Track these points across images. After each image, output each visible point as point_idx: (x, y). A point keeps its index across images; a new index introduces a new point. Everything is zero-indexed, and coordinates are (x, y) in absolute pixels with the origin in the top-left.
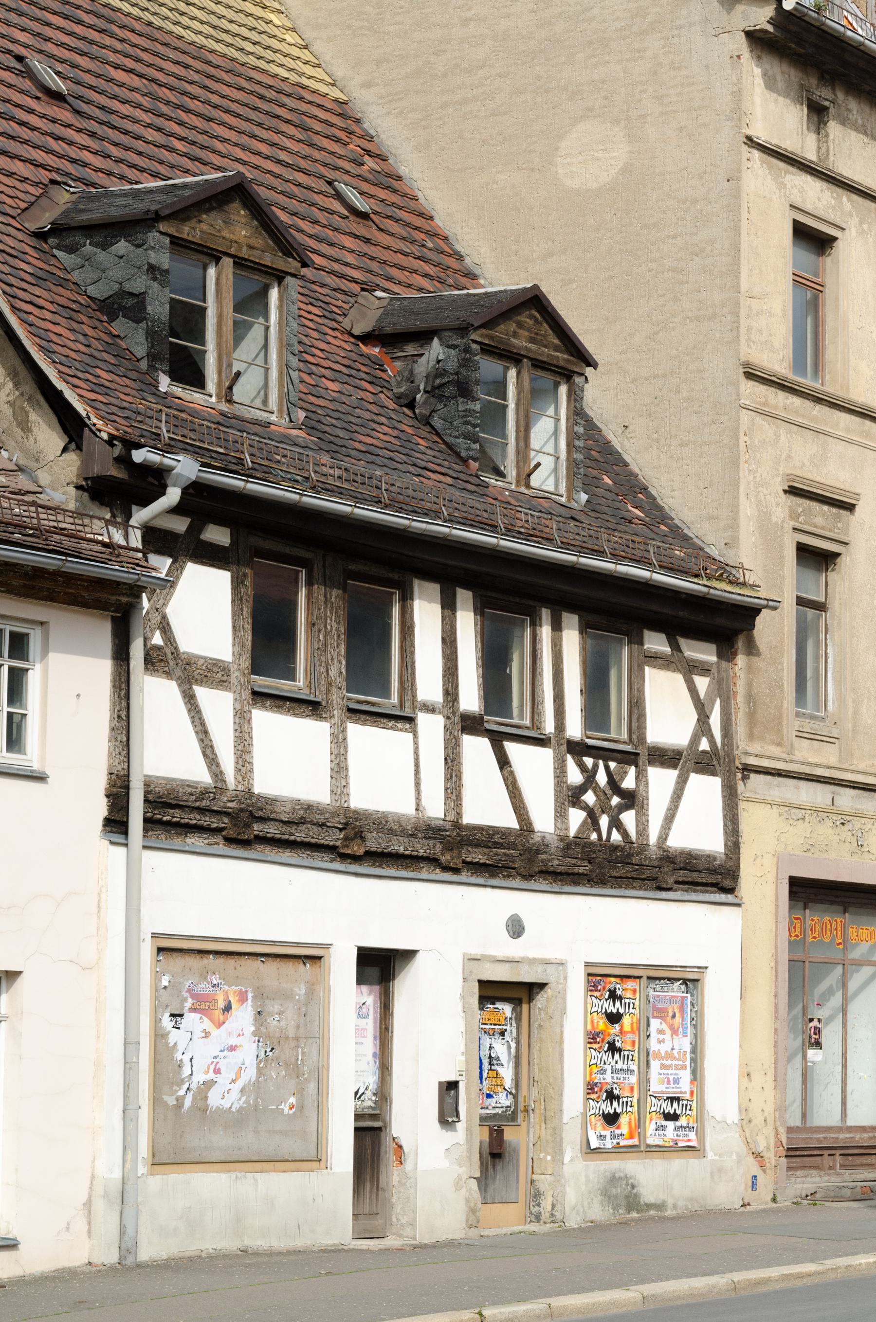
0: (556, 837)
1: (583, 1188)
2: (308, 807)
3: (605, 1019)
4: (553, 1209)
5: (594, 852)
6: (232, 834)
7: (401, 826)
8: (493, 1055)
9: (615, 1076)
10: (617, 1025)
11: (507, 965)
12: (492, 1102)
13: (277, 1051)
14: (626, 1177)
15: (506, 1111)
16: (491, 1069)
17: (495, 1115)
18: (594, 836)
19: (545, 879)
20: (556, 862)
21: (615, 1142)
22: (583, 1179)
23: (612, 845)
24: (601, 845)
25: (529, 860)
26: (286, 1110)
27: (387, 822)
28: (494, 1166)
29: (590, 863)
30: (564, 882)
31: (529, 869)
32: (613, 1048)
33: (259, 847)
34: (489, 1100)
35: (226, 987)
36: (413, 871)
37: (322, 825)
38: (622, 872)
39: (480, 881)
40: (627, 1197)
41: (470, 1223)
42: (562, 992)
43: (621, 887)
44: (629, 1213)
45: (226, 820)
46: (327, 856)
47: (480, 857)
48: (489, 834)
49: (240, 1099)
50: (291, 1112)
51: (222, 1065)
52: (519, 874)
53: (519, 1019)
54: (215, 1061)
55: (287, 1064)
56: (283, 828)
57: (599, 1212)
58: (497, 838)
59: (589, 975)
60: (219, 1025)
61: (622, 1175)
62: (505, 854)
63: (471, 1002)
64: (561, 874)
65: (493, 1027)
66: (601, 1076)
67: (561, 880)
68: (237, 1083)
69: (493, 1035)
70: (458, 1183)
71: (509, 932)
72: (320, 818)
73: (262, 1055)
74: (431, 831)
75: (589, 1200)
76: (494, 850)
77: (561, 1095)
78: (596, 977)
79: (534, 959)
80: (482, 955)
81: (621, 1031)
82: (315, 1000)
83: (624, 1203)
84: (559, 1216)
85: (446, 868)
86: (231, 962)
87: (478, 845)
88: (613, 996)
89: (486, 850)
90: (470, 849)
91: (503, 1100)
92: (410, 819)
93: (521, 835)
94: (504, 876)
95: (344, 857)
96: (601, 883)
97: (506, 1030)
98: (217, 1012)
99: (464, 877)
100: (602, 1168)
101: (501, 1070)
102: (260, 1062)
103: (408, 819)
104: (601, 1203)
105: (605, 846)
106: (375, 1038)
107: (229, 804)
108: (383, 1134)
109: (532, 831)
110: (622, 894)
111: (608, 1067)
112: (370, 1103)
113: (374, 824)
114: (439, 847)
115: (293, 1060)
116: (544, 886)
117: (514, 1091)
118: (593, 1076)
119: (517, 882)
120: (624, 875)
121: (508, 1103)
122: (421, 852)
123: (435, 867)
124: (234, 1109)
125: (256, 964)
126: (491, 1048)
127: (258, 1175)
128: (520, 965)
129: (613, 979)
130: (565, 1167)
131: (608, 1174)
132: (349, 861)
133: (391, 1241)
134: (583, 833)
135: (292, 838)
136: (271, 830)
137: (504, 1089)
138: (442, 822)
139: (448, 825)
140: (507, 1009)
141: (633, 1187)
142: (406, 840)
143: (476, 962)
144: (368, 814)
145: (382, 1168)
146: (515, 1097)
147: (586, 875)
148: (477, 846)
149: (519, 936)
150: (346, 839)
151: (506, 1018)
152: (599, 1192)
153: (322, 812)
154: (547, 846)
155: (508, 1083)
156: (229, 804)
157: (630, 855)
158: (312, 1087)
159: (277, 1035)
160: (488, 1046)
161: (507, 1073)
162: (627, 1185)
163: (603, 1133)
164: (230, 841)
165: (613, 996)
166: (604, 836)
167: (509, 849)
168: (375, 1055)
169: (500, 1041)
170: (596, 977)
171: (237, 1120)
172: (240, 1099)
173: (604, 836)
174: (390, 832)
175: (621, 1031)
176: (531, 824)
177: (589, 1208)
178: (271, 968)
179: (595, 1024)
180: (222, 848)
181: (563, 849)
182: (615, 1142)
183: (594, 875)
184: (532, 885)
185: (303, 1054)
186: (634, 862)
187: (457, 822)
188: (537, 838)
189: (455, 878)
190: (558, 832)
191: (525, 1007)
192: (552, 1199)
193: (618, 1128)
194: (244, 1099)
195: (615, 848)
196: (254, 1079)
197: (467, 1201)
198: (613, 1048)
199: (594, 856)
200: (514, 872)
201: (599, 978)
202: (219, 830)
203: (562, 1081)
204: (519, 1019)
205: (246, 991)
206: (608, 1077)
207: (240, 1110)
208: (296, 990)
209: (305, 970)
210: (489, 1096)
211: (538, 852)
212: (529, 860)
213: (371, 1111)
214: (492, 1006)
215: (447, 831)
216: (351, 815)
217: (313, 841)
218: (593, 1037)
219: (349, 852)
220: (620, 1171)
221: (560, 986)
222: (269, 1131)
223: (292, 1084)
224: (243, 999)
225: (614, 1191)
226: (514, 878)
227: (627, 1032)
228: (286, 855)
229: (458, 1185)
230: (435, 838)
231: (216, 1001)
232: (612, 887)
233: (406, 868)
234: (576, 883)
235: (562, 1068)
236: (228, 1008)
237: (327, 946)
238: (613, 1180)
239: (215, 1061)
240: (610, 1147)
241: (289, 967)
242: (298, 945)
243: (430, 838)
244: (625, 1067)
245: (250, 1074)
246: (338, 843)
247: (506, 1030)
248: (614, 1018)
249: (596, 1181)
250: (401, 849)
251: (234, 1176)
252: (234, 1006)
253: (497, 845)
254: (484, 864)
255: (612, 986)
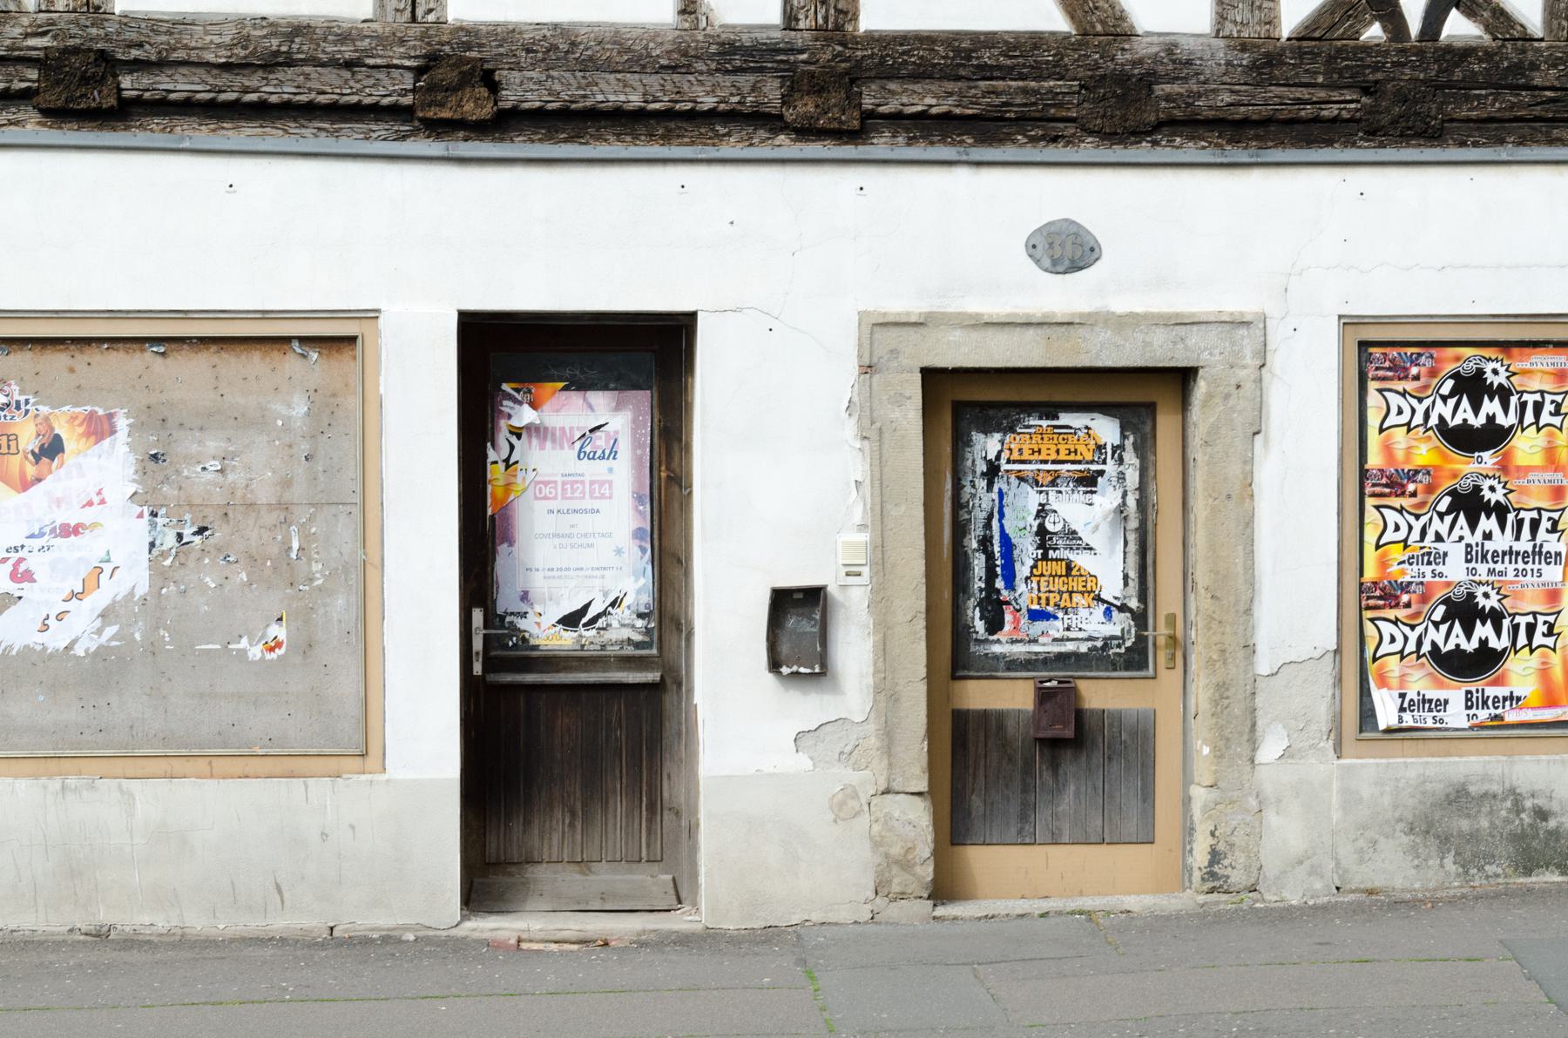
0: (1221, 43)
1: (1336, 816)
2: (299, 30)
3: (1436, 440)
4: (1211, 863)
5: (1376, 68)
6: (53, 99)
7: (629, 50)
8: (1049, 527)
9: (1482, 569)
10: (1486, 455)
11: (1031, 333)
12: (1055, 628)
13: (218, 535)
14: (1512, 791)
15: (1105, 646)
16: (1045, 557)
17: (1062, 658)
18: (1374, 32)
19: (1191, 138)
20: (1227, 98)
21: (1483, 714)
22: (1335, 799)
23: (1449, 49)
24: (1403, 51)
25: (1122, 98)
26: (256, 652)
27: (573, 44)
28: (1055, 767)
29: (1366, 91)
30: (1263, 141)
31: (1124, 118)
32: (1469, 504)
33: (156, 122)
34: (1040, 626)
35: (44, 410)
36: (692, 143)
37: (349, 65)
38: (1494, 108)
39: (1240, 155)
40: (1518, 838)
41: (896, 888)
42: (1249, 386)
43: (1501, 142)
44: (1528, 872)
45: (33, 74)
46: (380, 128)
47: (929, 101)
48: (957, 51)
49: (99, 632)
50: (273, 656)
51: (34, 562)
52: (1091, 133)
53: (1145, 449)
54: (14, 556)
55: (252, 560)
56: (224, 79)
57: (1395, 868)
58: (987, 57)
59: (1364, 345)
60: (25, 485)
61: (1495, 788)
62: (1025, 91)
63: (896, 414)
64: (1245, 122)
65: (1049, 467)
66: (1427, 569)
67: (1257, 137)
68: (88, 601)
69: (1053, 483)
70: (842, 804)
71: (1037, 262)
72: (347, 52)
73: (170, 541)
74: (738, 54)
75: (1361, 843)
76: (982, 83)
77: (1248, 611)
78: (1376, 353)
79: (1133, 316)
80: (930, 315)
81: (1504, 466)
82: (345, 427)
83: (1504, 850)
84: (1237, 877)
85: (806, 132)
86: (58, 360)
87: (922, 73)
88: (1472, 387)
89: (950, 86)
90: (892, 86)
91: (1093, 625)
92: (657, 34)
93: (1076, 47)
94: (1034, 140)
95: (438, 128)
96: (1418, 135)
97: (1101, 473)
98: (15, 461)
99: (880, 146)
100: (1412, 774)
101: (1081, 560)
102: (164, 555)
103: (655, 35)
104: (1413, 850)
105: (1420, 52)
106: (639, 499)
107: (31, 42)
108: (669, 699)
109: (1129, 35)
110: (1504, 157)
111: (1456, 553)
112: (626, 633)
113: (528, 51)
114: (772, 92)
115: (274, 550)
116: (1191, 152)
117: (1134, 603)
118: (1394, 568)
119: (1088, 150)
120: (1507, 115)
121: (1113, 629)
122: (708, 102)
123: (775, 131)
124: (79, 651)
125: (148, 356)
126: (1042, 512)
127: (135, 785)
128: (1081, 331)
129: (1468, 352)
130: (1262, 773)
131: (1439, 788)
132: (461, 134)
133: (681, 922)
134: (1331, 28)
135: (253, 97)
136: (180, 85)
137: (1098, 599)
138: (778, 34)
139: (799, 39)
140: (1106, 430)
141: (1542, 814)
142: (653, 81)
143: (911, 330)
144: (506, 35)
145: (668, 766)
146: (1140, 618)
147: (1358, 121)
148: (916, 77)
149: (1076, 267)
150: (432, 88)
151: (1100, 448)
152: (1400, 826)
153: (345, 37)
154: (1189, 62)
155: (1112, 588)
156: (31, 42)
157: (1518, 68)
158: (340, 605)
159: (219, 498)
160: (1034, 509)
161: (1107, 566)
162: (1518, 809)
163: (1432, 694)
164: (58, 115)
165: (1472, 387)
166: (1414, 26)
167: (1038, 78)
168: (638, 534)
169: (1080, 495)
170: (1376, 353)
171: (101, 671)
172: (99, 632)
173: (1414, 26)
174: (589, 65)
175: (1504, 466)
176: (1122, 17)
177: (1361, 861)
178: (197, 364)
179: (1400, 455)
180: (32, 127)
181: (1253, 67)
182: (1483, 714)
183: (1385, 120)
184: (1142, 152)
185: (306, 537)
186: (1537, 81)
187: (838, 28)
188: (1142, 48)
189: (848, 151)
190: (1229, 28)
191: (1166, 424)
192: (1211, 841)
193: (1498, 682)
194: (111, 631)
195: (1462, 54)
196: (143, 588)
197: (877, 843)
198: (1469, 504)
199: (1379, 76)
200: (1070, 130)
201: (1410, 350)
202: (25, 96)
203: (1251, 583)
204: (1145, 449)
205: (110, 416)
206: (1455, 570)
207: (101, 654)
208: (278, 407)
209: (313, 368)
210: (1035, 616)
211: (1150, 79)
212: (1122, 98)
213: (630, 651)
214: (1045, 423)
215: (801, 52)
216: (445, 38)
217: (322, 99)
218: (1370, 484)
219: (446, 114)
220: (1486, 778)
221: (1242, 373)
222: (202, 695)
223: (274, 601)
224: (99, 429)
225: (1465, 825)
226: (1070, 141)
227: (1529, 469)
228: (246, 134)
229: (843, 807)
230: (761, 70)
231: (12, 438)
232: (1463, 144)
233: (666, 139)
234: (1309, 142)
235: (1250, 554)
236: (52, 449)
237: (372, 315)
238: (1459, 797)
239: (14, 556)
240: (1464, 723)
241: (255, 363)
242: (265, 315)
243: (737, 71)
244: (1524, 545)
245: (134, 577)
246: (407, 100)
247: (1101, 473)
248: (1463, 439)
249: (1386, 800)
250: (635, 100)
251: (56, 784)
252: (69, 445)
253: (986, 72)
254: (947, 117)
255: (1469, 368)
